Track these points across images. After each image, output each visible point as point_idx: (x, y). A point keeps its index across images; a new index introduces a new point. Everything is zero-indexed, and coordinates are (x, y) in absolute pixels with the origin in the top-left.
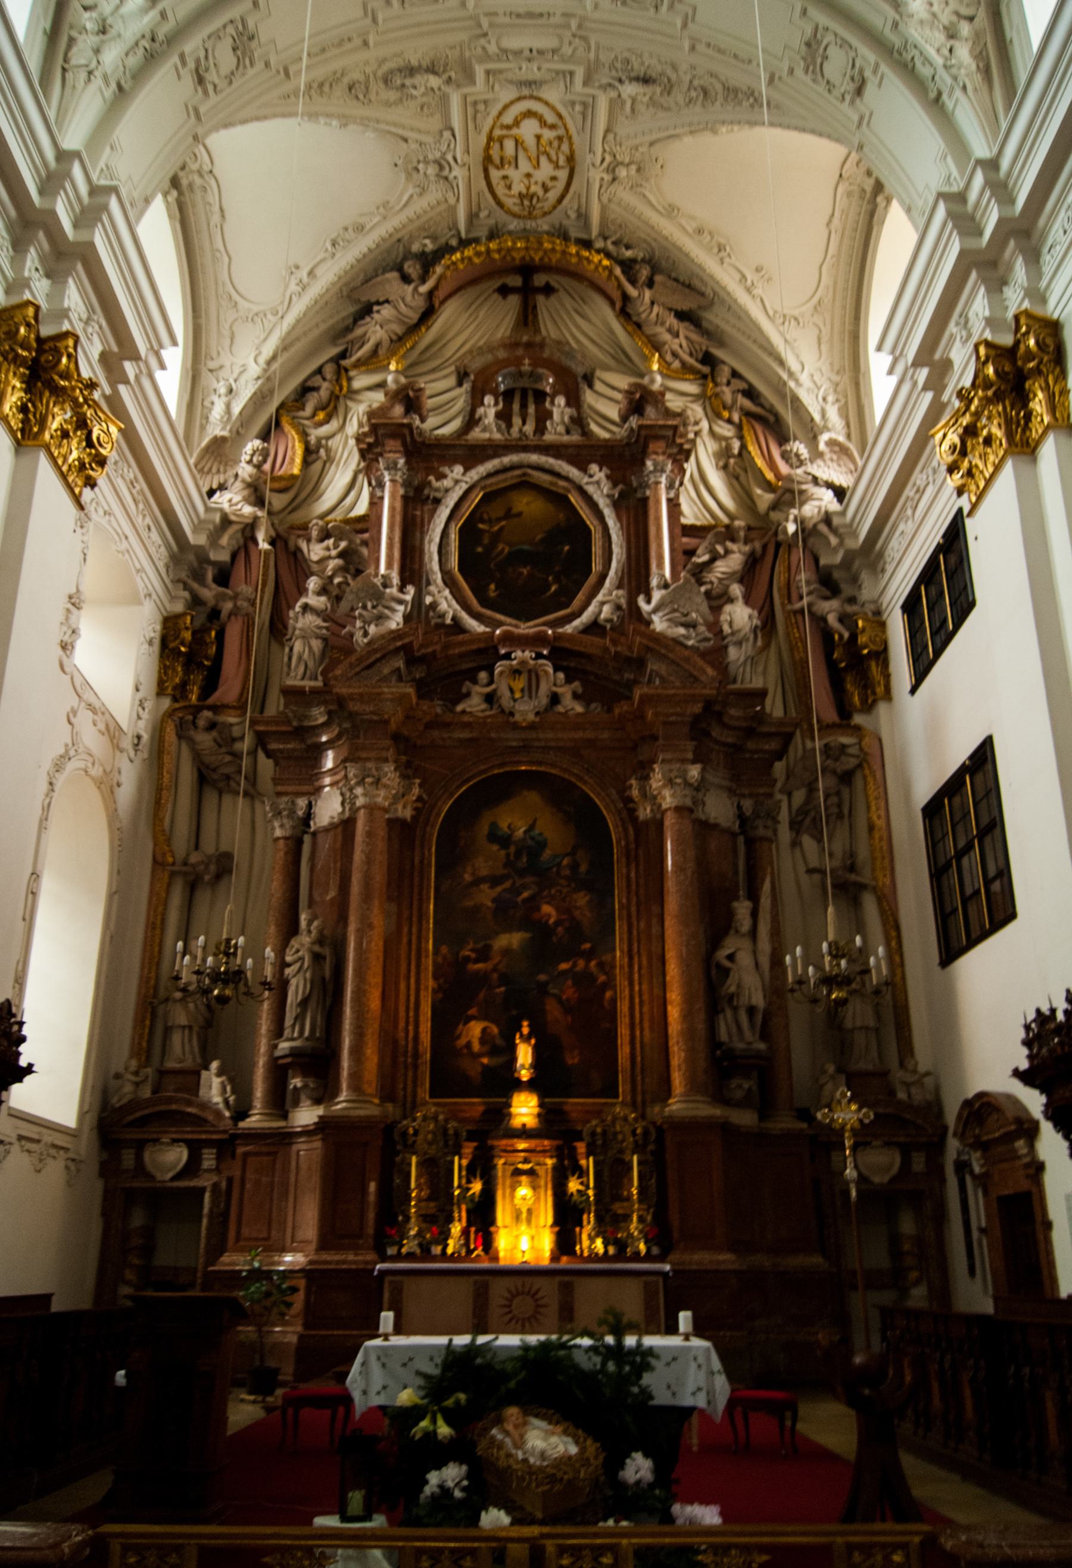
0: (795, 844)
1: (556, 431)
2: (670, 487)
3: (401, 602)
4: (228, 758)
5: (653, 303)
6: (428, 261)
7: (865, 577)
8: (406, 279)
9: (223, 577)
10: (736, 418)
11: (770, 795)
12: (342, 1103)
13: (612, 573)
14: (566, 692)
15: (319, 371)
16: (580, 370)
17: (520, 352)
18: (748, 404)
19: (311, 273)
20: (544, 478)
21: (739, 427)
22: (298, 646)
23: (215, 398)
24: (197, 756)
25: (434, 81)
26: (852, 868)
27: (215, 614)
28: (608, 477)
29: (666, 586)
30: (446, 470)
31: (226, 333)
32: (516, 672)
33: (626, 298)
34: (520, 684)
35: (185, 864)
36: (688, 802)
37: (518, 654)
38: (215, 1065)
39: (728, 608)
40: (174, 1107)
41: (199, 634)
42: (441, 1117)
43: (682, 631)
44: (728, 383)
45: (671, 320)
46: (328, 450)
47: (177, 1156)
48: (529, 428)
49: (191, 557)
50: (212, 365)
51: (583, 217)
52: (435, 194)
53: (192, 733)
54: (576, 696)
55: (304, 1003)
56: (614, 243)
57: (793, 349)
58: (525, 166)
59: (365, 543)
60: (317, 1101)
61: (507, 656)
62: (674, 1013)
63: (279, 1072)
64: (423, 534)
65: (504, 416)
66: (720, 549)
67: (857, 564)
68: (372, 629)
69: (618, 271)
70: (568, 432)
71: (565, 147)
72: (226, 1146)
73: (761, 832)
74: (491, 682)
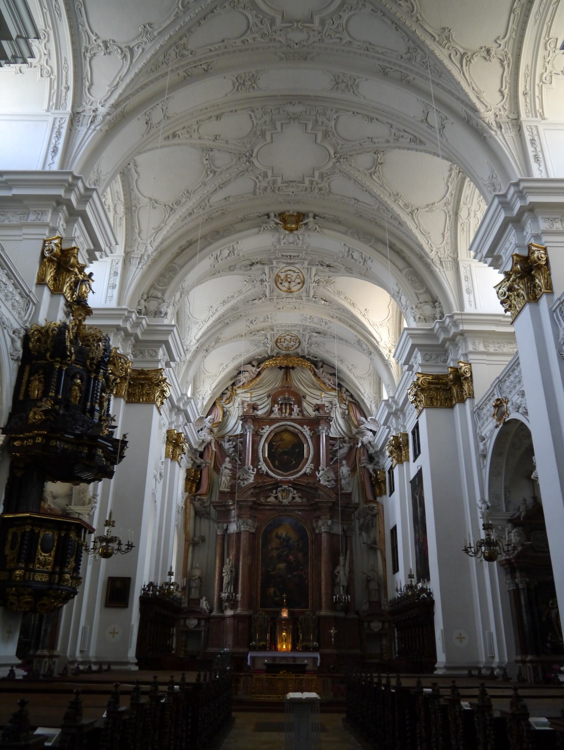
0: (360, 534)
1: (295, 416)
2: (327, 431)
3: (253, 474)
4: (203, 509)
6: (260, 362)
7: (381, 457)
8: (253, 366)
9: (202, 455)
10: (347, 403)
11: (351, 524)
12: (239, 611)
13: (310, 458)
14: (296, 495)
15: (227, 389)
16: (302, 395)
17: (285, 389)
18: (351, 399)
19: (226, 366)
20: (292, 429)
21: (348, 406)
22: (223, 478)
23: (199, 401)
24: (195, 509)
25: (263, 332)
26: (375, 543)
27: (199, 466)
28: (309, 429)
29: (323, 470)
30: (264, 427)
32: (283, 491)
33: (315, 372)
34: (284, 494)
35: (193, 540)
36: (328, 530)
37: (284, 486)
38: (204, 598)
39: (342, 468)
40: (194, 609)
41: (195, 475)
42: (264, 614)
43: (327, 483)
45: (329, 376)
46: (229, 412)
47: (194, 622)
48: (287, 415)
49: (193, 451)
50: (198, 390)
51: (303, 351)
53: (194, 502)
54: (299, 497)
55: (228, 583)
58: (286, 342)
59: (241, 442)
60: (232, 609)
61: (281, 487)
62: (323, 588)
63: (220, 600)
64: (258, 445)
65: (280, 410)
66: (341, 445)
67: (378, 454)
68: (246, 483)
69: (313, 366)
70: (298, 415)
72: (208, 619)
73: (349, 535)
74: (276, 493)
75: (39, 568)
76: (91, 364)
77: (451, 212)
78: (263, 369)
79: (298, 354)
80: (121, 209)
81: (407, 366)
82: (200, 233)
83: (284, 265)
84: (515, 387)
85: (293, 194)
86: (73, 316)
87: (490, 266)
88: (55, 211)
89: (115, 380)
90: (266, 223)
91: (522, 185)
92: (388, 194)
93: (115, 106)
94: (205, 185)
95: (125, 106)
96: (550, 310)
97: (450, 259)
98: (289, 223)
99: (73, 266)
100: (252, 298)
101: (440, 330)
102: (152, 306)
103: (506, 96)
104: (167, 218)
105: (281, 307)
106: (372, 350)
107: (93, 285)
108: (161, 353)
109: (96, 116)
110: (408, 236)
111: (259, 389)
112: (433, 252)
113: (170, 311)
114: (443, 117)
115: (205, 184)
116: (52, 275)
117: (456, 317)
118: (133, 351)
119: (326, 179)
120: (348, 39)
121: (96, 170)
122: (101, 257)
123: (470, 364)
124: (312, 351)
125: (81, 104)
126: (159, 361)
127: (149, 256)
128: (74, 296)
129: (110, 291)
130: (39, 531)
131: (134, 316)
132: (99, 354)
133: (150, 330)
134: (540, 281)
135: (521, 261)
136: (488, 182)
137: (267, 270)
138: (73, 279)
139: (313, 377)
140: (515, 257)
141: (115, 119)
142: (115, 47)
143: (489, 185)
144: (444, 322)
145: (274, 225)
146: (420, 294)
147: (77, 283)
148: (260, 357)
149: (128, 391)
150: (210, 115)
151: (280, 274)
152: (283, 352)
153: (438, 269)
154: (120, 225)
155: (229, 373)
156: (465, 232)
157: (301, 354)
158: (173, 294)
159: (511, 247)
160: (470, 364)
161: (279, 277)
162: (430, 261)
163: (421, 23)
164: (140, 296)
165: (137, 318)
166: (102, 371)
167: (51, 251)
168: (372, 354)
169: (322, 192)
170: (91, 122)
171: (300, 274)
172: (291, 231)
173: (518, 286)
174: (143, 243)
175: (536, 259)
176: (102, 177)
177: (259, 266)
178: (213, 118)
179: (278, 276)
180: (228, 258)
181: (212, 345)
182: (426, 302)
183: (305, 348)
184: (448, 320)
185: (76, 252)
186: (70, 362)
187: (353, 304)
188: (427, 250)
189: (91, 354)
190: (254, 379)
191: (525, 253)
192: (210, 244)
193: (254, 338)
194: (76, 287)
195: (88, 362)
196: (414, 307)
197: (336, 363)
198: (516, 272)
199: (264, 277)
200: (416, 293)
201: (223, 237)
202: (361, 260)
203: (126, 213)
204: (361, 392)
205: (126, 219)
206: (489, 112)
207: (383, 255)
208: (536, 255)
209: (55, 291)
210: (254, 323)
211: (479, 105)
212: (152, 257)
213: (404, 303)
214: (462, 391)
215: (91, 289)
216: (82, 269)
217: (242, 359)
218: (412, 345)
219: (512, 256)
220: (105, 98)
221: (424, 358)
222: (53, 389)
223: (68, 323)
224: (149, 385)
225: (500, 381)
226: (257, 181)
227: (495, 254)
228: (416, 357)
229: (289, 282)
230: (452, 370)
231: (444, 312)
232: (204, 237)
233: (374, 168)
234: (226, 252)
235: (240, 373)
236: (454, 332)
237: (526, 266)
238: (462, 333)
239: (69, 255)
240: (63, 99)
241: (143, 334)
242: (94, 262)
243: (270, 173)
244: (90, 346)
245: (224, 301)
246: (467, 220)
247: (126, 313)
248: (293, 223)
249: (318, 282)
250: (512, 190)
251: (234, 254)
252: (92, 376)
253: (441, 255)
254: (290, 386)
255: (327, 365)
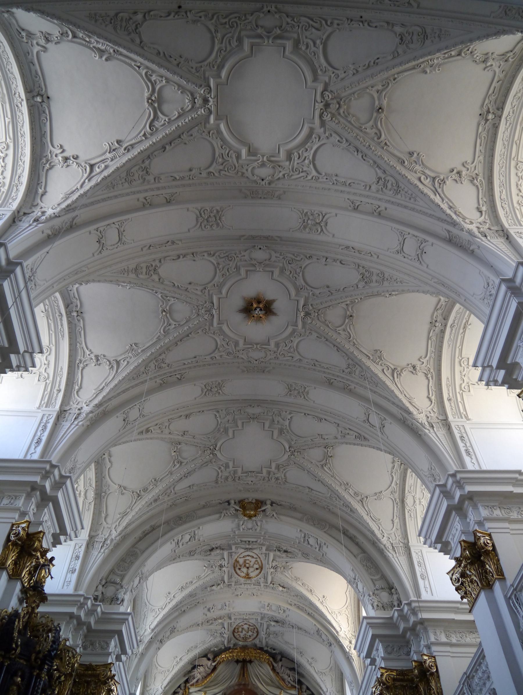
5: (282, 666)
6: (216, 654)
8: (209, 659)
15: (179, 687)
17: (241, 687)
19: (181, 659)
25: (220, 621)
31: (153, 678)
33: (273, 666)
44: (306, 692)
45: (288, 672)
50: (148, 689)
52: (219, 639)
56: (270, 648)
57: (324, 683)
58: (244, 632)
69: (271, 659)
71: (256, 630)
76: (36, 659)
77: (398, 500)
78: (219, 663)
79: (255, 645)
80: (91, 495)
81: (369, 660)
82: (163, 518)
83: (243, 550)
84: (485, 684)
85: (252, 483)
86: (26, 603)
87: (440, 551)
88: (29, 496)
89: (59, 677)
90: (226, 509)
91: (459, 476)
92: (339, 484)
93: (98, 406)
94: (171, 474)
95: (107, 406)
96: (505, 596)
97: (401, 544)
98: (249, 510)
99: (36, 550)
100: (211, 584)
101: (399, 618)
102: (110, 591)
103: (433, 401)
104: (133, 503)
105: (239, 593)
106: (332, 640)
107: (53, 570)
108: (113, 645)
109: (80, 413)
110: (360, 523)
111: (214, 687)
112: (385, 538)
113: (127, 597)
114: (382, 418)
115: (171, 473)
116: (13, 559)
117: (414, 605)
118: (83, 643)
119: (282, 470)
120: (299, 357)
121: (73, 460)
122: (65, 541)
123: (434, 657)
124: (270, 642)
125: (69, 404)
126: (109, 654)
127: (112, 540)
128: (32, 581)
129: (69, 575)
131: (89, 603)
132: (47, 646)
133: (105, 618)
134: (490, 567)
135: (469, 547)
136: (428, 473)
137: (226, 557)
138: (34, 564)
139: (271, 673)
140: (462, 543)
141: (96, 416)
142: (105, 360)
143: (429, 475)
144: (402, 610)
145: (234, 512)
146: (376, 580)
147: (38, 567)
148: (216, 649)
149: (72, 691)
150: (180, 414)
151: (239, 559)
152: (240, 643)
153: (391, 555)
154: (88, 510)
155: (184, 666)
156: (413, 519)
157: (259, 645)
158: (132, 580)
159: (458, 533)
160: (434, 657)
161: (238, 562)
162: (382, 547)
163: (357, 346)
164: (99, 581)
165: (93, 605)
166: (46, 667)
167: (17, 535)
168: (333, 646)
169: (279, 481)
170: (75, 418)
171: (258, 559)
172: (250, 517)
173: (470, 572)
174: (108, 528)
175: (483, 545)
176: (77, 465)
177: (218, 551)
178: (183, 417)
179: (237, 561)
180: (189, 543)
181: (167, 636)
182: (382, 589)
183: (263, 639)
184: (406, 608)
185: (41, 536)
186: (13, 657)
187: (311, 591)
188: (379, 536)
189: (38, 646)
190: (209, 675)
191: (471, 539)
192: (172, 529)
193: (212, 627)
194: (35, 571)
195: (33, 657)
196: (371, 593)
197: (296, 655)
198: (466, 558)
199: (223, 563)
200: (372, 579)
201: (185, 522)
202: (316, 546)
203: (95, 499)
204: (323, 690)
205: (95, 504)
206: (421, 414)
207: (338, 540)
208: (482, 541)
209: (13, 576)
210: (212, 611)
211: (411, 409)
212: (115, 542)
213: (361, 590)
214: (430, 690)
215: (50, 574)
216: (44, 553)
217: (196, 652)
218: (373, 635)
219: (460, 542)
220: (91, 399)
221: (386, 651)
223: (20, 611)
224: (96, 683)
225: (468, 677)
226: (219, 471)
227: (444, 540)
228: (377, 650)
229: (248, 568)
230: (416, 664)
231: (402, 599)
232: (167, 522)
233: (325, 460)
234: (187, 537)
235: (194, 667)
236: (414, 621)
237: (474, 552)
238: (422, 622)
239: (34, 539)
240: (54, 398)
241: (96, 622)
242: (58, 546)
243: (231, 464)
244: (39, 637)
245: (182, 588)
246: (413, 507)
247: (82, 599)
248: (252, 510)
249: (275, 568)
250: (450, 481)
251: (195, 540)
252: (35, 674)
253: (393, 540)
254: (247, 683)
255: (286, 658)
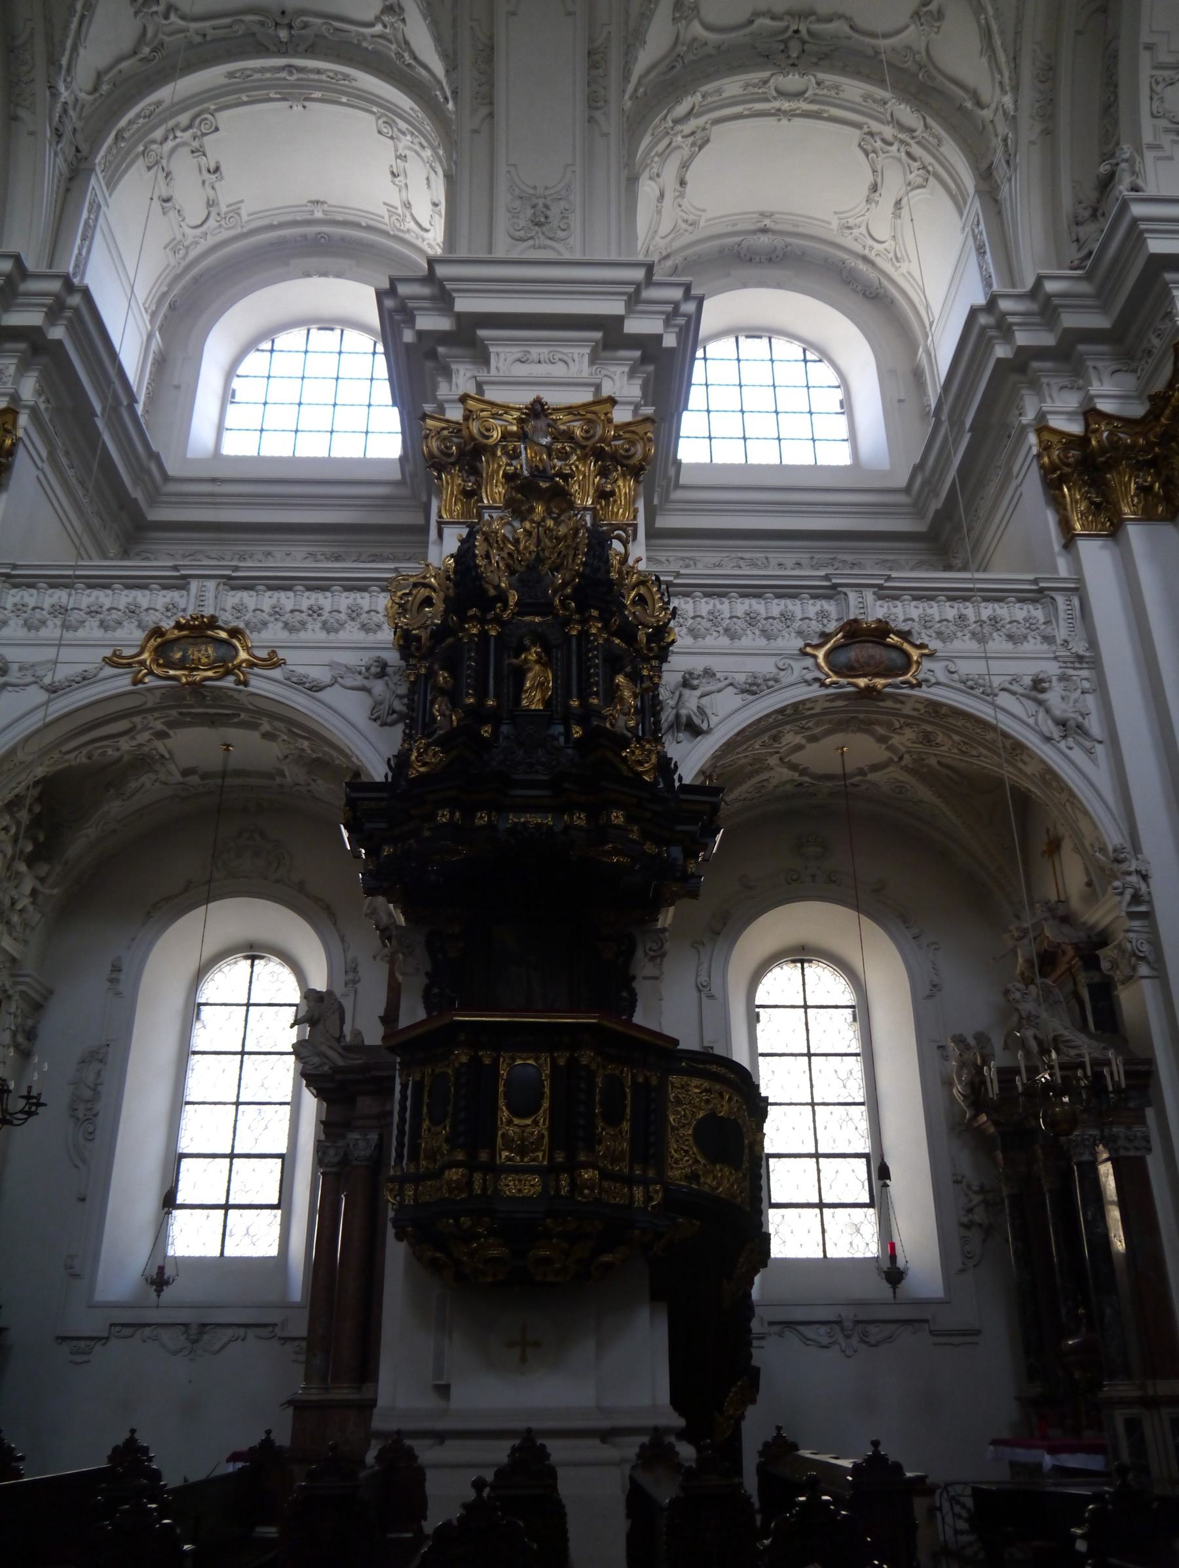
75: (509, 1159)
130: (496, 1062)
222: (469, 686)
